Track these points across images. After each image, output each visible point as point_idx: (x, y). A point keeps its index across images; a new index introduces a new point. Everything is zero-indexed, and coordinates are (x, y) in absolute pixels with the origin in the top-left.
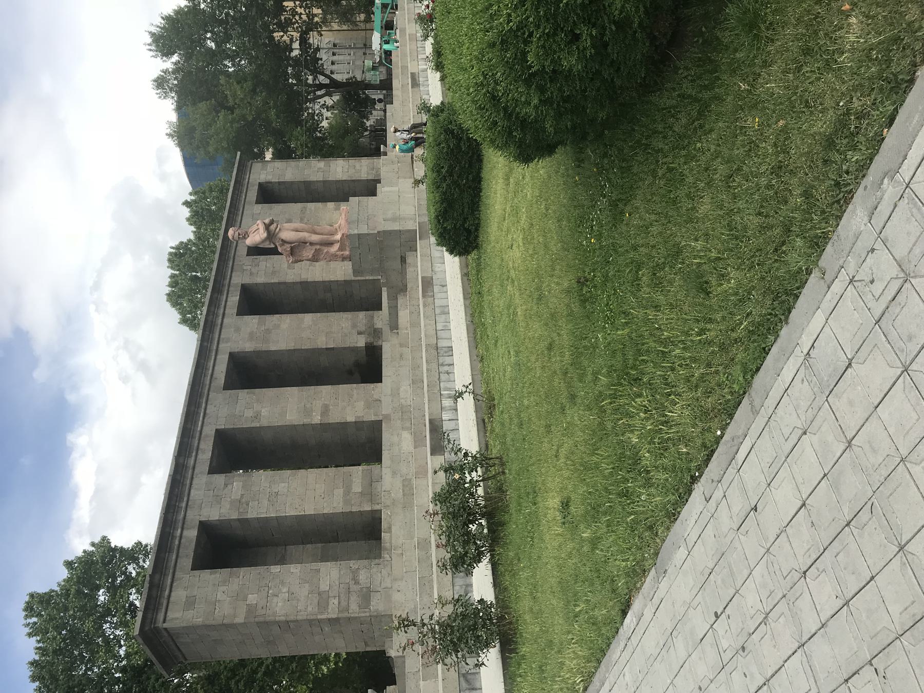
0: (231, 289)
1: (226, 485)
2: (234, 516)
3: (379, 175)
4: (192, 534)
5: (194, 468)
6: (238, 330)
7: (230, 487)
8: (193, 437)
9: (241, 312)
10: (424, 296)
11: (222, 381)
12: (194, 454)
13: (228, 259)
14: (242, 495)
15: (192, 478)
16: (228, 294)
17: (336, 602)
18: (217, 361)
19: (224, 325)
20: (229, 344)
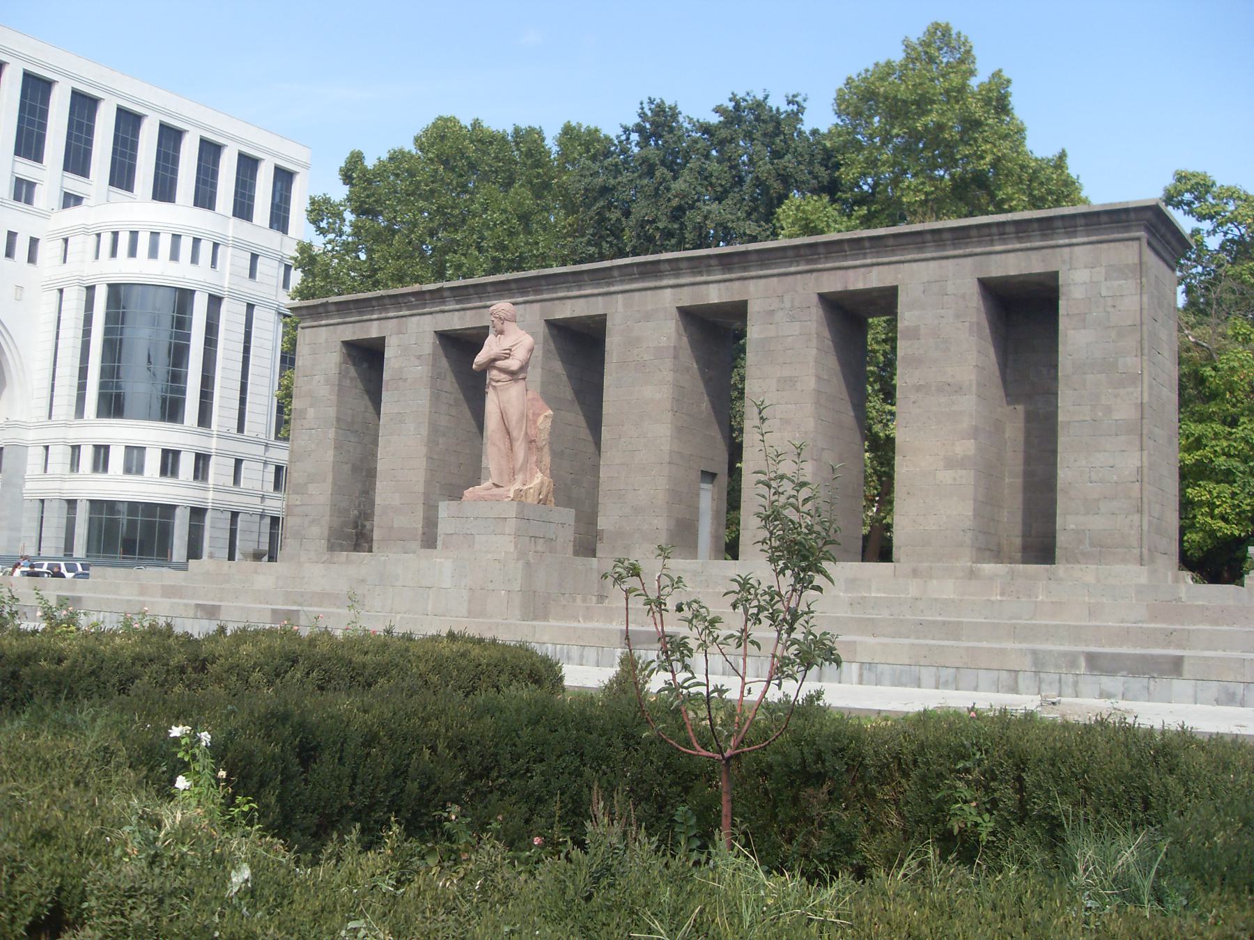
0: (737, 283)
1: (419, 357)
2: (386, 376)
3: (1073, 559)
4: (373, 331)
5: (443, 312)
6: (647, 317)
7: (417, 362)
8: (481, 299)
9: (691, 316)
10: (198, 606)
11: (559, 315)
12: (458, 307)
13: (809, 262)
14: (405, 380)
15: (431, 313)
16: (725, 281)
17: (298, 503)
18: (593, 299)
19: (660, 292)
20: (620, 308)
